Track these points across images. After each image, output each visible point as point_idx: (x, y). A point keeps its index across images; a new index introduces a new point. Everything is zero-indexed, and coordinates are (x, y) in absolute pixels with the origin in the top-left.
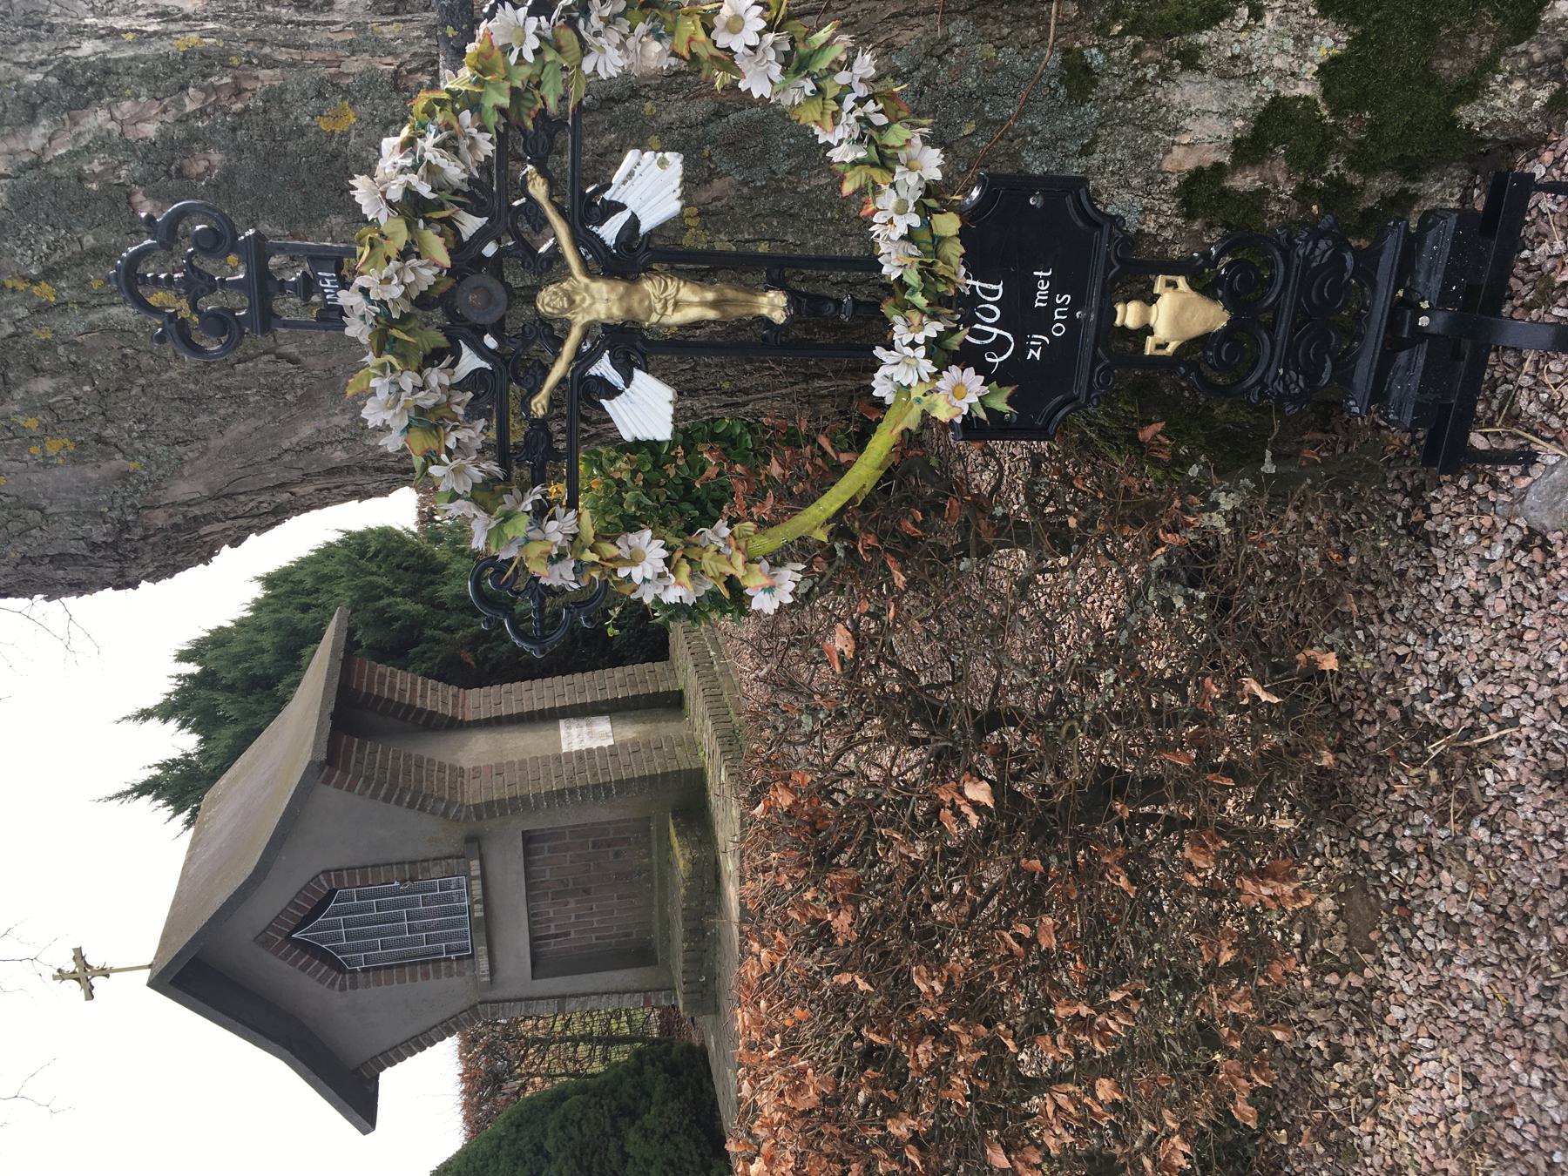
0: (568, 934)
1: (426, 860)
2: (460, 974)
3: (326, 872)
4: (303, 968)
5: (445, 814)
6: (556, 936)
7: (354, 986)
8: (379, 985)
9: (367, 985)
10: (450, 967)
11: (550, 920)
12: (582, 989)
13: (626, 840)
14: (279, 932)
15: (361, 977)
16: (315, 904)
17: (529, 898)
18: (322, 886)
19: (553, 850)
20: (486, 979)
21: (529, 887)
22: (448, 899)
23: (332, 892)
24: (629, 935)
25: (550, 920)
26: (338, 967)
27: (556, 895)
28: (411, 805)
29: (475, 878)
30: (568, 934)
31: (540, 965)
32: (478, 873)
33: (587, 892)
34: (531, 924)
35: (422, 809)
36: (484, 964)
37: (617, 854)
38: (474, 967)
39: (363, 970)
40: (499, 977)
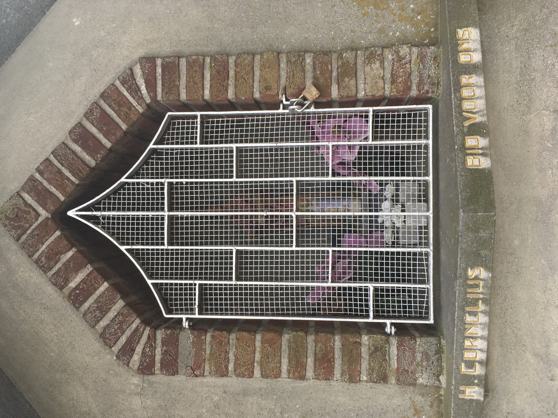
1: (354, 49)
2: (406, 378)
3: (148, 61)
4: (77, 298)
7: (170, 366)
8: (222, 373)
9: (196, 370)
10: (378, 352)
15: (187, 339)
18: (135, 90)
26: (143, 305)
29: (470, 69)
32: (477, 57)
38: (437, 361)
39: (195, 324)
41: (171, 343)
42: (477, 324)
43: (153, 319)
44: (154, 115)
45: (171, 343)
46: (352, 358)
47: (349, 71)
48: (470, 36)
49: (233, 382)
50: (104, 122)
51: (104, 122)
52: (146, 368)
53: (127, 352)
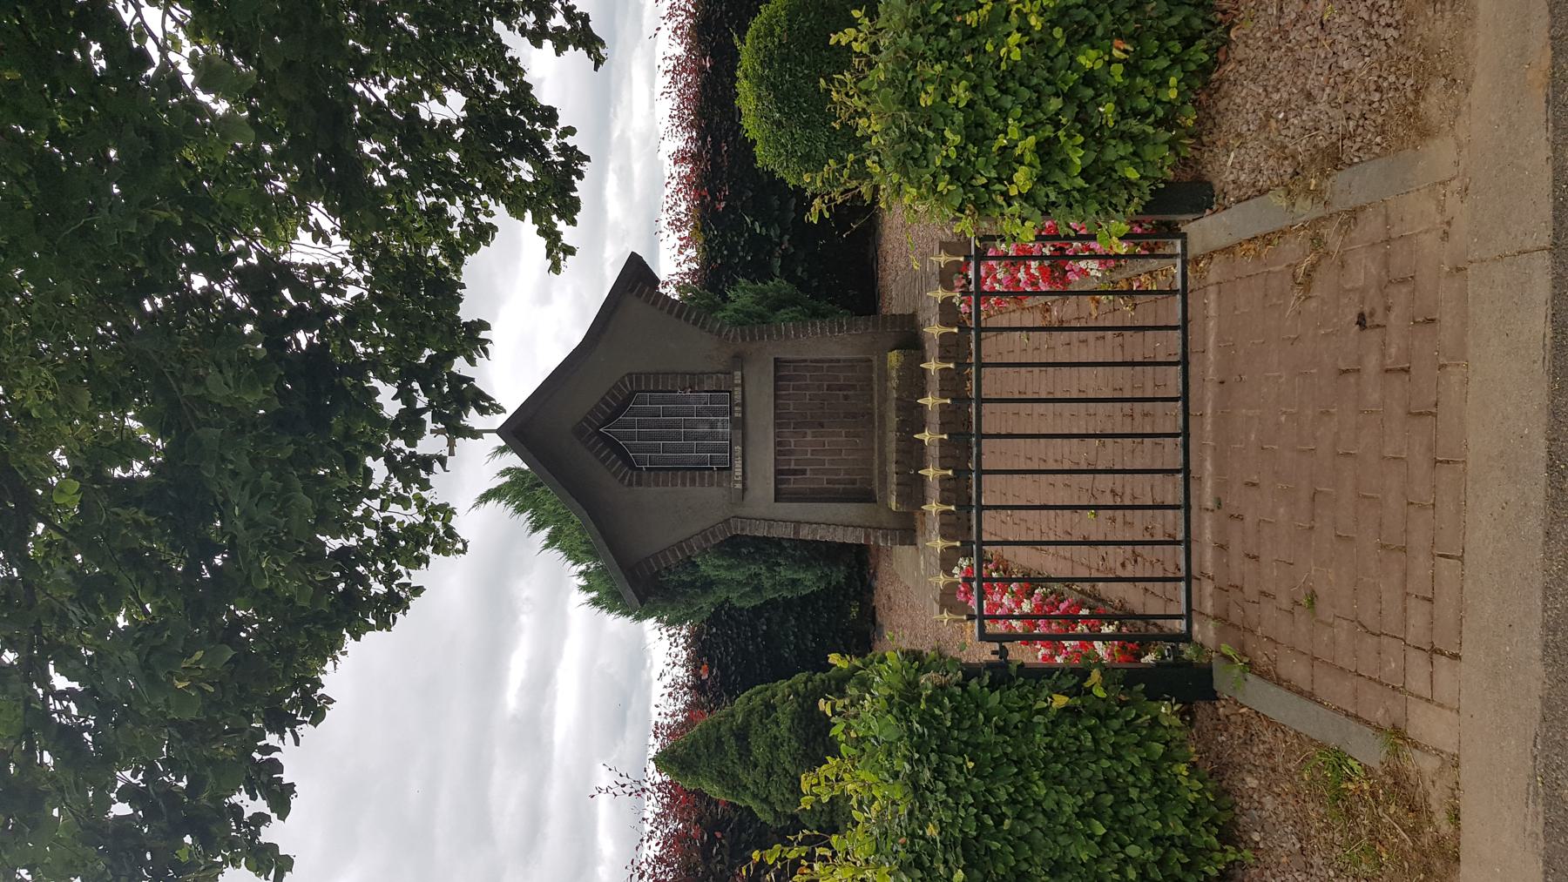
0: (803, 472)
1: (703, 373)
2: (720, 485)
4: (603, 461)
5: (719, 333)
6: (795, 472)
7: (639, 484)
10: (711, 476)
11: (791, 452)
12: (812, 518)
13: (853, 387)
14: (590, 424)
15: (645, 475)
16: (617, 405)
17: (777, 425)
19: (796, 388)
20: (739, 486)
21: (777, 416)
22: (714, 436)
23: (632, 394)
24: (853, 482)
25: (791, 452)
27: (797, 425)
28: (695, 323)
30: (803, 472)
31: (779, 496)
33: (822, 425)
34: (778, 453)
35: (703, 327)
36: (738, 471)
37: (846, 397)
40: (749, 496)
41: (639, 476)
42: (738, 464)
43: (632, 468)
44: (632, 394)
45: (639, 476)
46: (702, 478)
47: (701, 382)
48: (738, 374)
49: (661, 489)
50: (614, 397)
51: (614, 397)
52: (630, 484)
53: (624, 478)
